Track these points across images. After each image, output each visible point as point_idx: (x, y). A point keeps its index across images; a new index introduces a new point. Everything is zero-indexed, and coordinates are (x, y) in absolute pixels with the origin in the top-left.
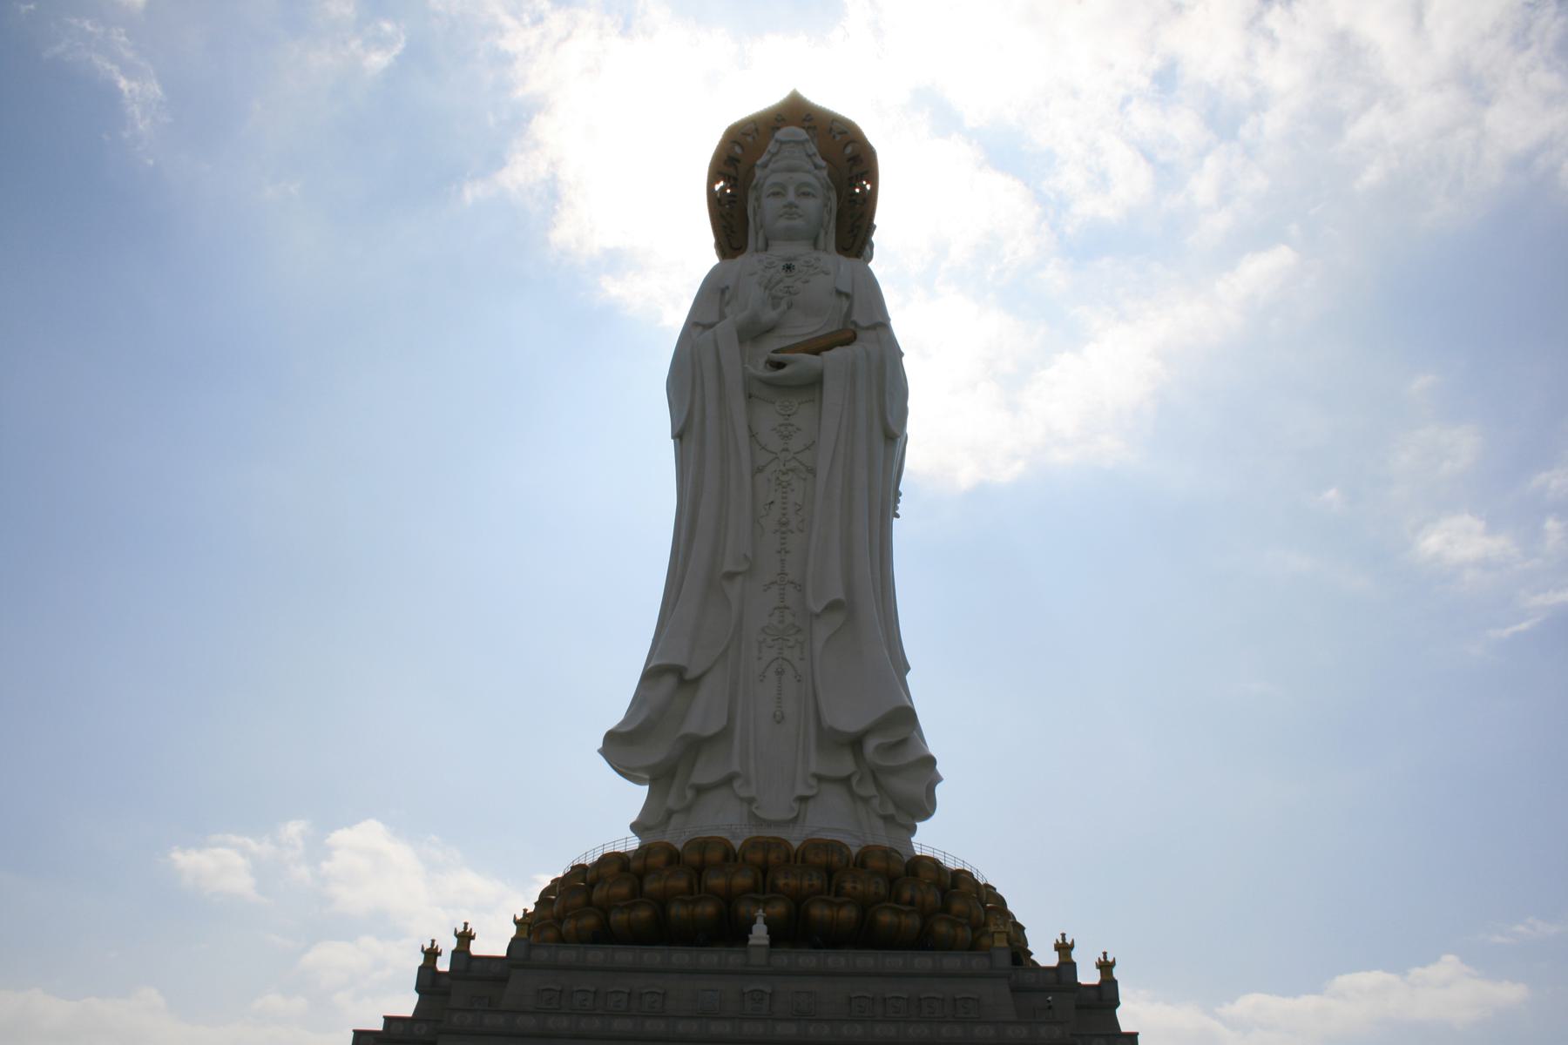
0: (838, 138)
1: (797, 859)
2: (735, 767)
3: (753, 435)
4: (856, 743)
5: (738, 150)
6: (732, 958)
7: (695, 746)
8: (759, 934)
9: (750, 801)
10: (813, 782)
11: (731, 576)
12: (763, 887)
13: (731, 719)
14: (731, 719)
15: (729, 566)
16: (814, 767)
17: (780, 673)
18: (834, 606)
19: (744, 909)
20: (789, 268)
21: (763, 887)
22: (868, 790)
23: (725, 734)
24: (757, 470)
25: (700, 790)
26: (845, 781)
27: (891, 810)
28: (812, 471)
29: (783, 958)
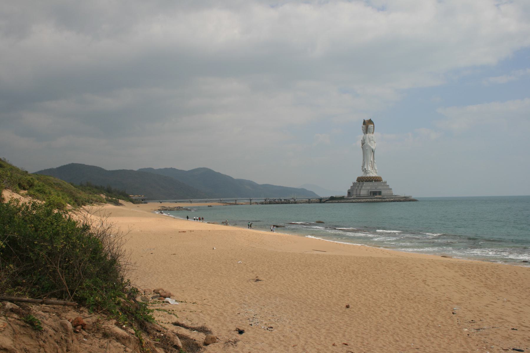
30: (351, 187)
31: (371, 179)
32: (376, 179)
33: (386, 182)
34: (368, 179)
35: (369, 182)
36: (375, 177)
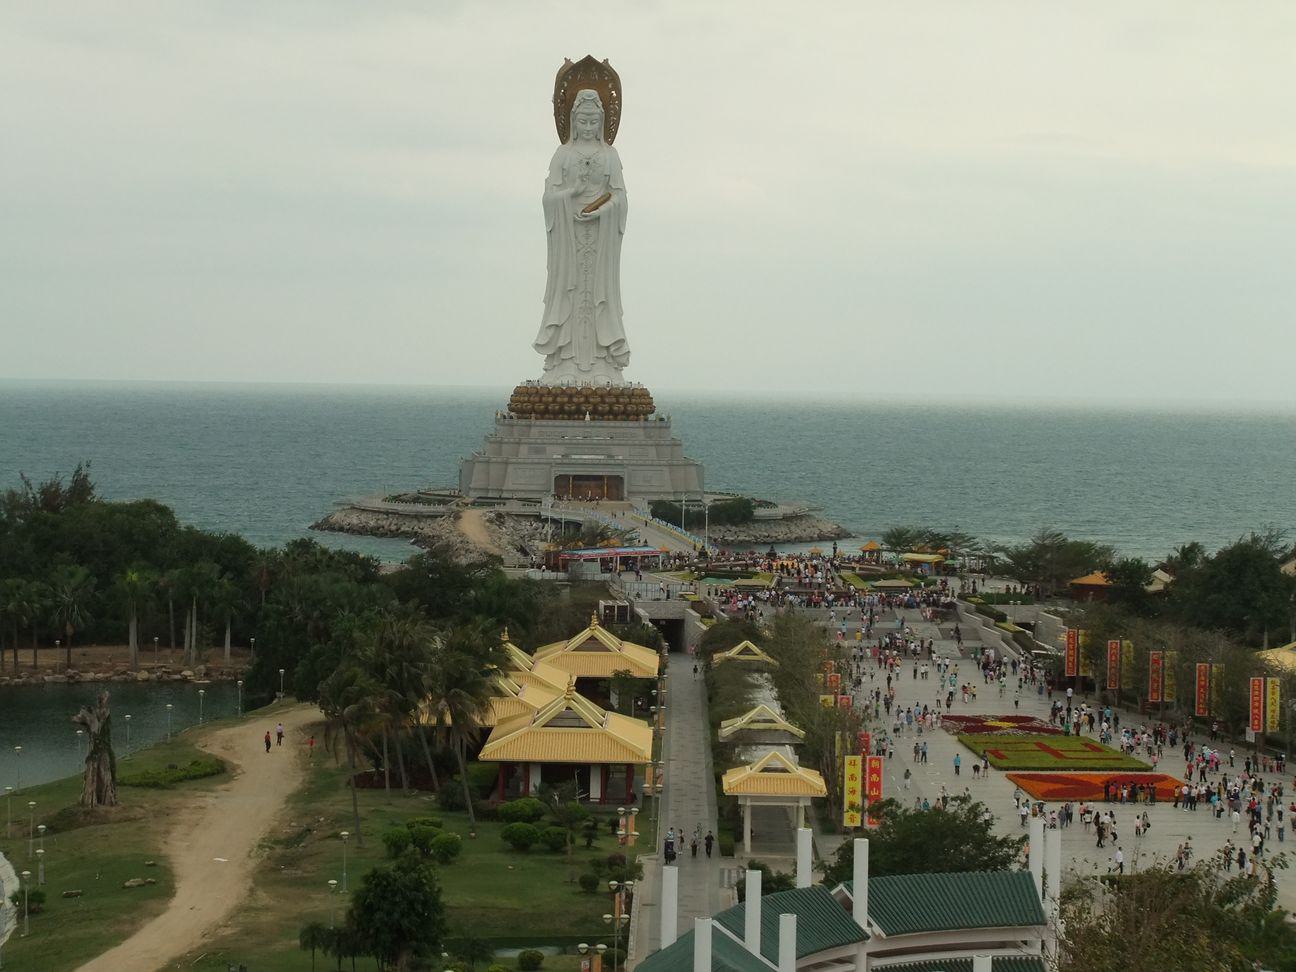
1: (595, 393)
3: (576, 238)
4: (608, 348)
6: (581, 423)
7: (561, 348)
8: (588, 416)
11: (570, 290)
12: (587, 401)
17: (585, 322)
18: (602, 302)
21: (587, 401)
22: (611, 361)
23: (570, 343)
26: (604, 358)
29: (593, 423)
31: (570, 401)
32: (618, 402)
35: (557, 423)
36: (609, 394)
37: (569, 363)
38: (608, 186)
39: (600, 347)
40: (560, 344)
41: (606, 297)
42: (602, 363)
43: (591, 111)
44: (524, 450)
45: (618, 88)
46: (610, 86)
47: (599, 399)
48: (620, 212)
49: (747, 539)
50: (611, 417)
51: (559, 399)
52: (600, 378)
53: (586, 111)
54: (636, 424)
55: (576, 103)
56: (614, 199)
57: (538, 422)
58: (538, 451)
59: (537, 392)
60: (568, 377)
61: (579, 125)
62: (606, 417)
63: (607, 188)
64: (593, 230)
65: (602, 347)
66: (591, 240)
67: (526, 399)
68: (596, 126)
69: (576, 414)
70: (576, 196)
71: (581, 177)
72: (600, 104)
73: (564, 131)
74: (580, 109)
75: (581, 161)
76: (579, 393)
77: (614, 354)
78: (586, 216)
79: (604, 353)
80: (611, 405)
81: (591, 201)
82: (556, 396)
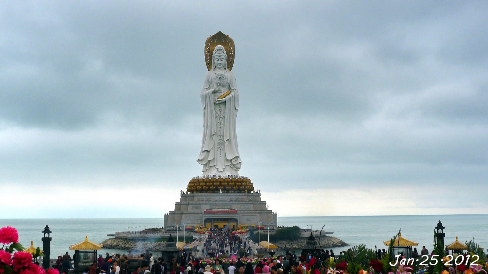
0: (228, 41)
2: (215, 164)
4: (231, 160)
5: (210, 45)
6: (218, 194)
7: (209, 161)
8: (221, 191)
9: (217, 169)
10: (225, 166)
12: (221, 184)
13: (214, 157)
14: (214, 157)
15: (212, 134)
16: (225, 164)
17: (220, 149)
18: (228, 140)
19: (219, 187)
20: (220, 78)
21: (221, 184)
22: (233, 166)
23: (214, 159)
24: (216, 117)
25: (210, 166)
27: (235, 169)
28: (224, 117)
29: (223, 194)
30: (177, 204)
32: (235, 185)
33: (258, 194)
34: (213, 185)
37: (213, 168)
38: (229, 88)
39: (227, 160)
40: (209, 159)
41: (230, 138)
42: (228, 168)
43: (221, 55)
44: (190, 207)
45: (233, 45)
46: (229, 45)
47: (226, 183)
48: (235, 99)
49: (297, 247)
50: (232, 191)
51: (207, 184)
52: (228, 174)
53: (219, 55)
54: (244, 194)
55: (214, 52)
56: (232, 93)
57: (197, 195)
58: (197, 208)
59: (198, 182)
60: (213, 173)
61: (216, 61)
62: (230, 191)
63: (229, 89)
64: (222, 107)
65: (229, 160)
66: (222, 113)
67: (193, 184)
68: (224, 61)
69: (216, 190)
70: (215, 92)
71: (217, 84)
72: (225, 52)
73: (209, 64)
74: (216, 54)
75: (217, 77)
76: (217, 181)
77: (234, 163)
78: (219, 101)
79: (229, 163)
80: (232, 186)
81: (222, 94)
82: (206, 182)
